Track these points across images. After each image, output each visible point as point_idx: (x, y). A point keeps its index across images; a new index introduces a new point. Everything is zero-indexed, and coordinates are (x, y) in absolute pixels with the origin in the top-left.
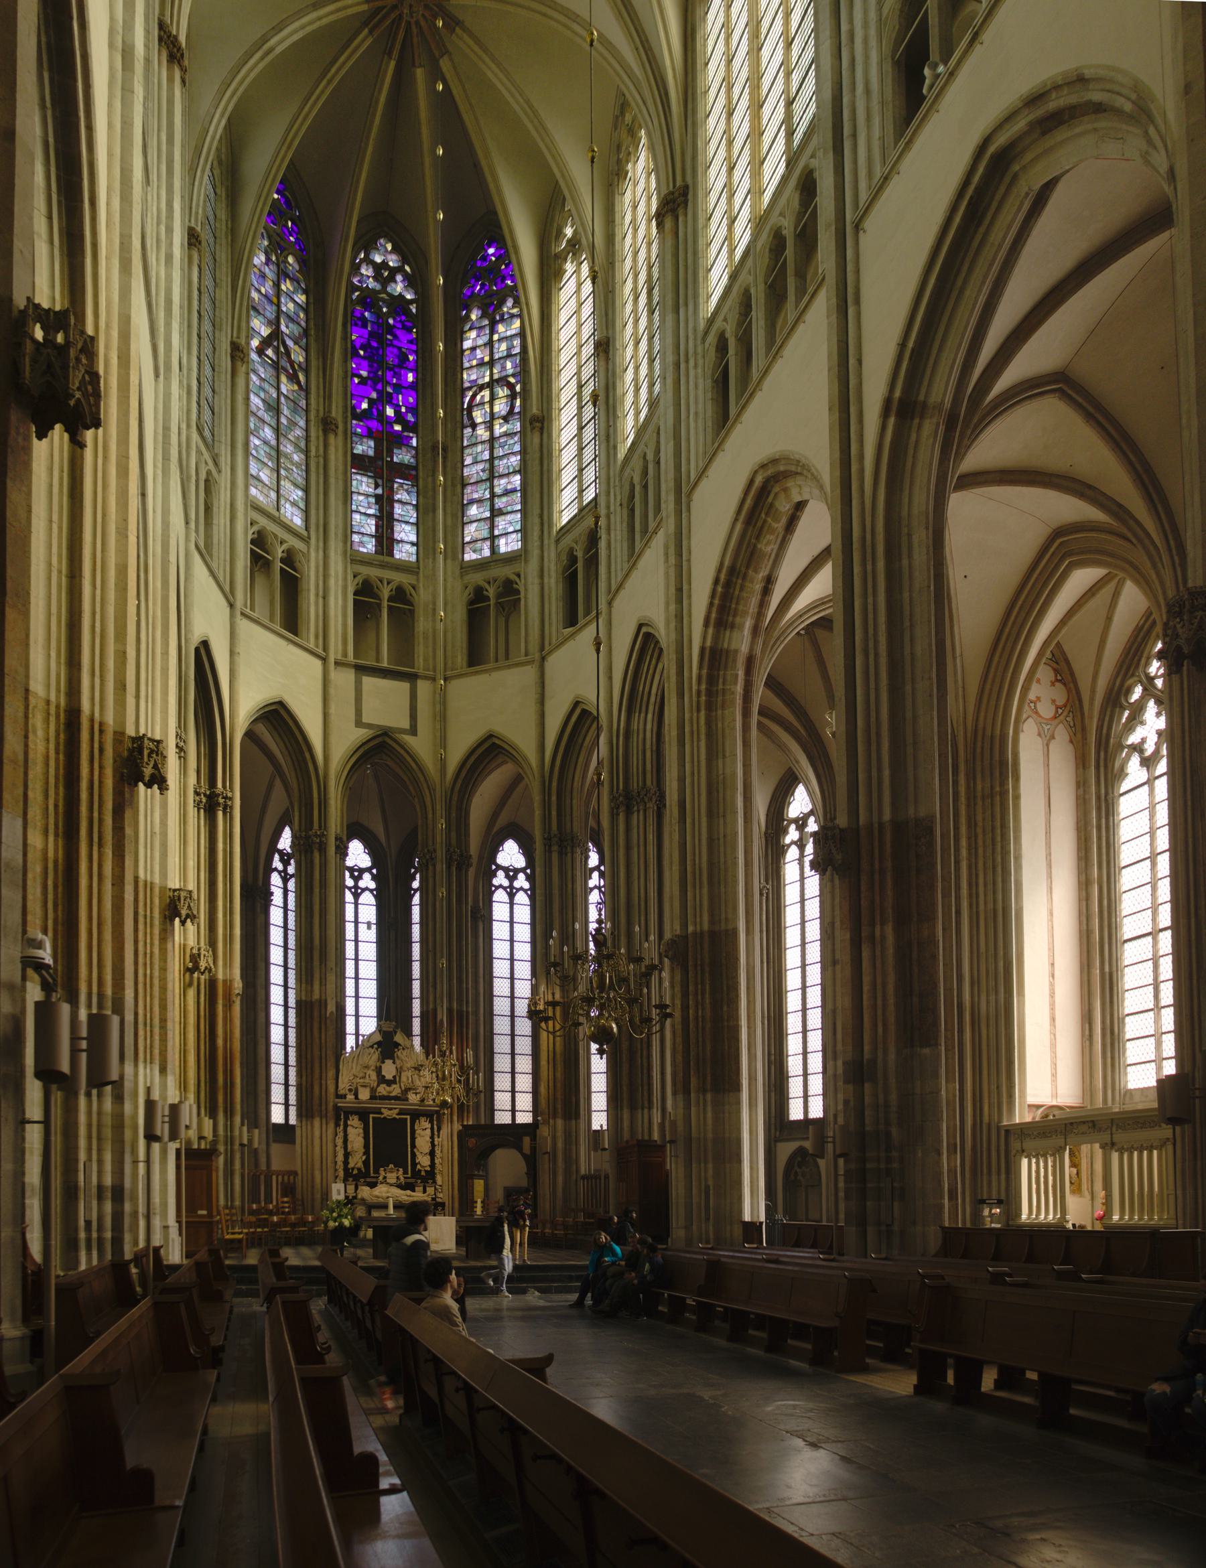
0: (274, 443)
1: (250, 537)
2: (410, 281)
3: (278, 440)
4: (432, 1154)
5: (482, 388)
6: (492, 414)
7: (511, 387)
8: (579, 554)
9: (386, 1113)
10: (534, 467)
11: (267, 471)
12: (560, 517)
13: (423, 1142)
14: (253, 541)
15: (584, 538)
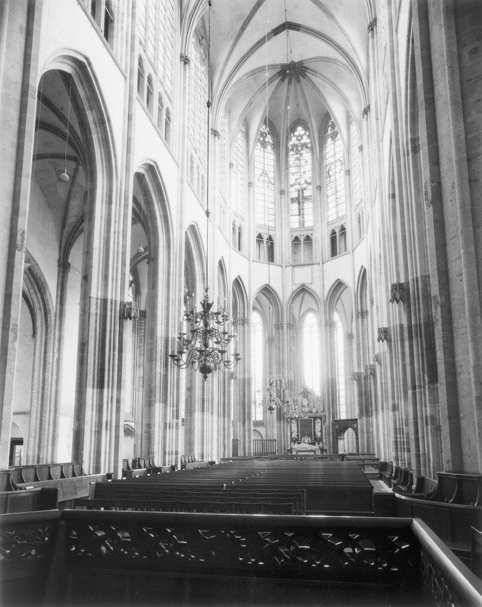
2: (309, 136)
5: (332, 164)
6: (336, 173)
7: (341, 161)
10: (348, 188)
13: (318, 428)
14: (257, 237)
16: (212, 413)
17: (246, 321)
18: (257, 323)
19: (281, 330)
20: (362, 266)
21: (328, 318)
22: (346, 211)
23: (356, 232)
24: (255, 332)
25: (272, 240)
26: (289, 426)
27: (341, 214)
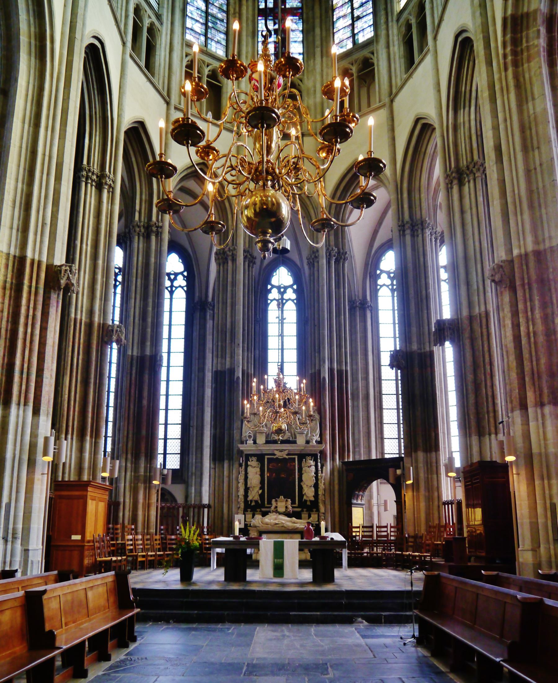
0: (203, 8)
1: (185, 64)
3: (207, 7)
4: (316, 486)
8: (413, 21)
9: (279, 455)
11: (199, 25)
12: (399, 5)
15: (416, 9)
16: (36, 412)
17: (154, 229)
18: (176, 274)
19: (230, 263)
20: (417, 120)
21: (332, 243)
22: (376, 30)
23: (399, 64)
24: (171, 292)
25: (219, 82)
26: (242, 470)
27: (361, 39)
